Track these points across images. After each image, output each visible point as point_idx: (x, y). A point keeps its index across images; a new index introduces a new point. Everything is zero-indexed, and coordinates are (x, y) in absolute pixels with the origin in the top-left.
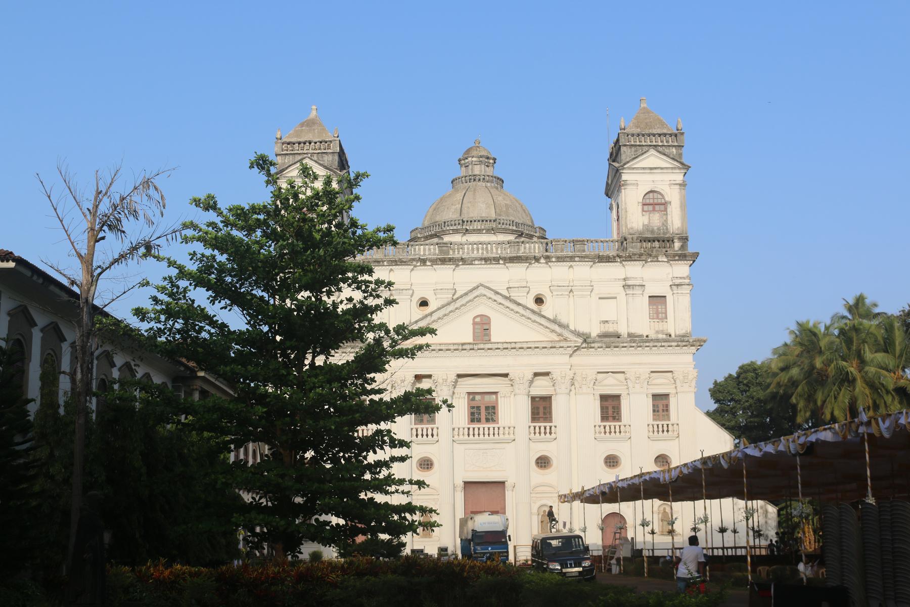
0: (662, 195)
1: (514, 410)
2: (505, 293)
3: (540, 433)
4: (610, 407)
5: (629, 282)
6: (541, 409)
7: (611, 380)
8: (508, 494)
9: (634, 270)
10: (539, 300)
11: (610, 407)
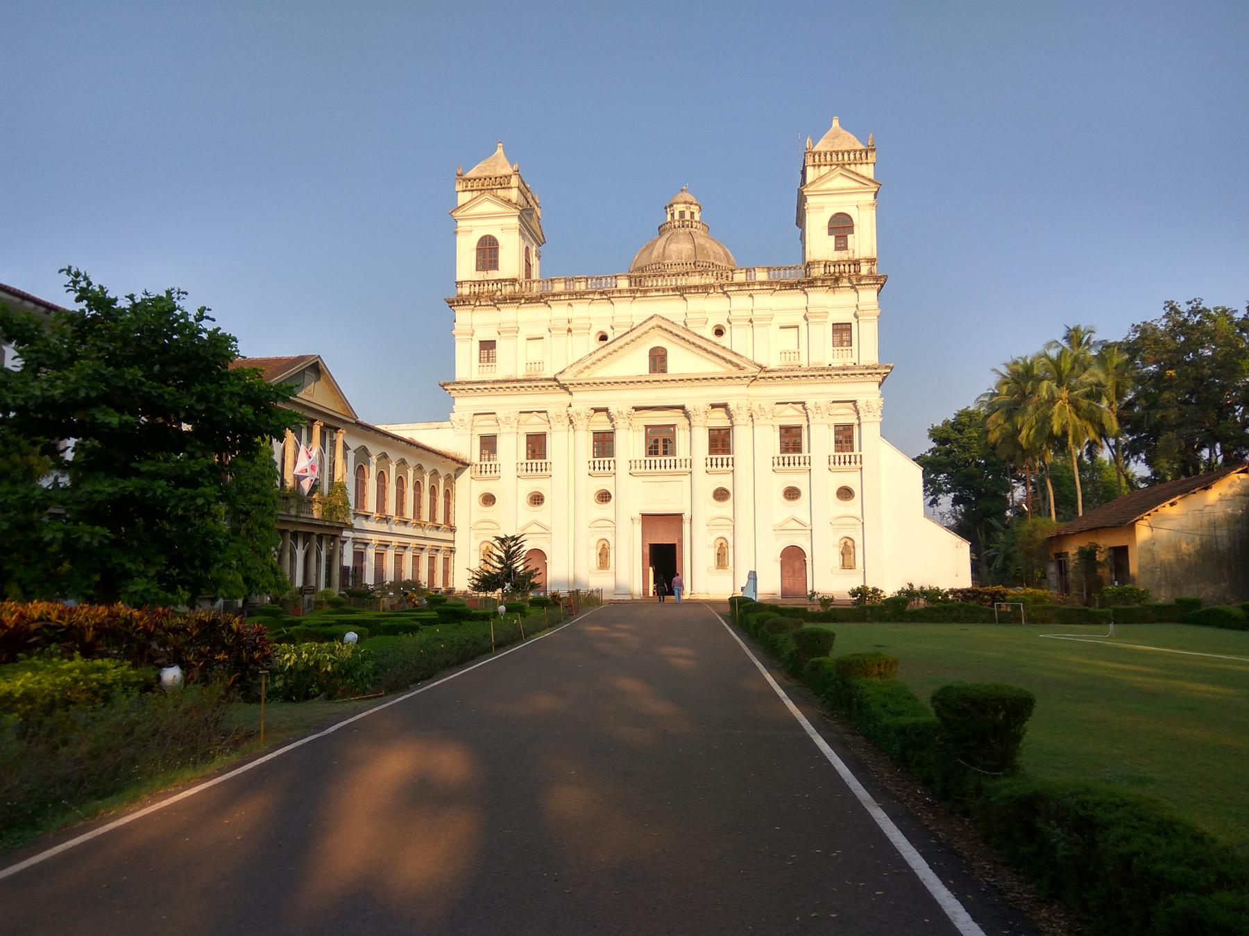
4: (791, 439)
6: (720, 442)
8: (686, 527)
10: (719, 332)
11: (791, 439)
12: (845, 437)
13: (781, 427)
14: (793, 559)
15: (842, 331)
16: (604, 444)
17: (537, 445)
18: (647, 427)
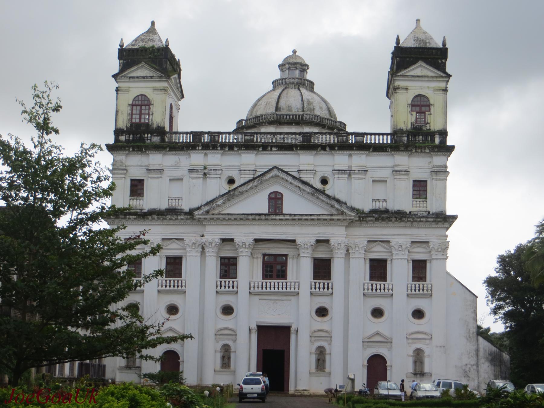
0: (427, 98)
1: (301, 270)
2: (296, 174)
3: (319, 288)
4: (378, 270)
5: (397, 169)
6: (322, 269)
7: (378, 248)
9: (402, 160)
10: (324, 181)
11: (378, 270)
13: (372, 261)
14: (377, 367)
16: (228, 268)
17: (174, 266)
18: (264, 255)
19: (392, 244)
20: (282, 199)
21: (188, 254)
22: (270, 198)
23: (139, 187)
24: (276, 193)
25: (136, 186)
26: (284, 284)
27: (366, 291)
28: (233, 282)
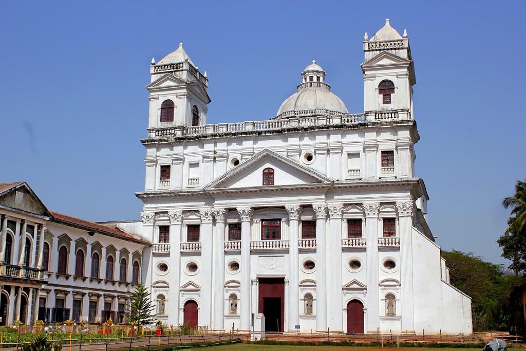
1: (291, 232)
4: (355, 227)
6: (309, 229)
8: (286, 287)
9: (371, 136)
10: (309, 158)
11: (355, 227)
12: (389, 224)
14: (355, 310)
15: (387, 157)
16: (235, 231)
17: (194, 232)
19: (364, 205)
20: (273, 173)
21: (203, 222)
22: (264, 174)
23: (167, 172)
24: (268, 169)
25: (165, 171)
26: (278, 243)
27: (344, 246)
28: (237, 243)
